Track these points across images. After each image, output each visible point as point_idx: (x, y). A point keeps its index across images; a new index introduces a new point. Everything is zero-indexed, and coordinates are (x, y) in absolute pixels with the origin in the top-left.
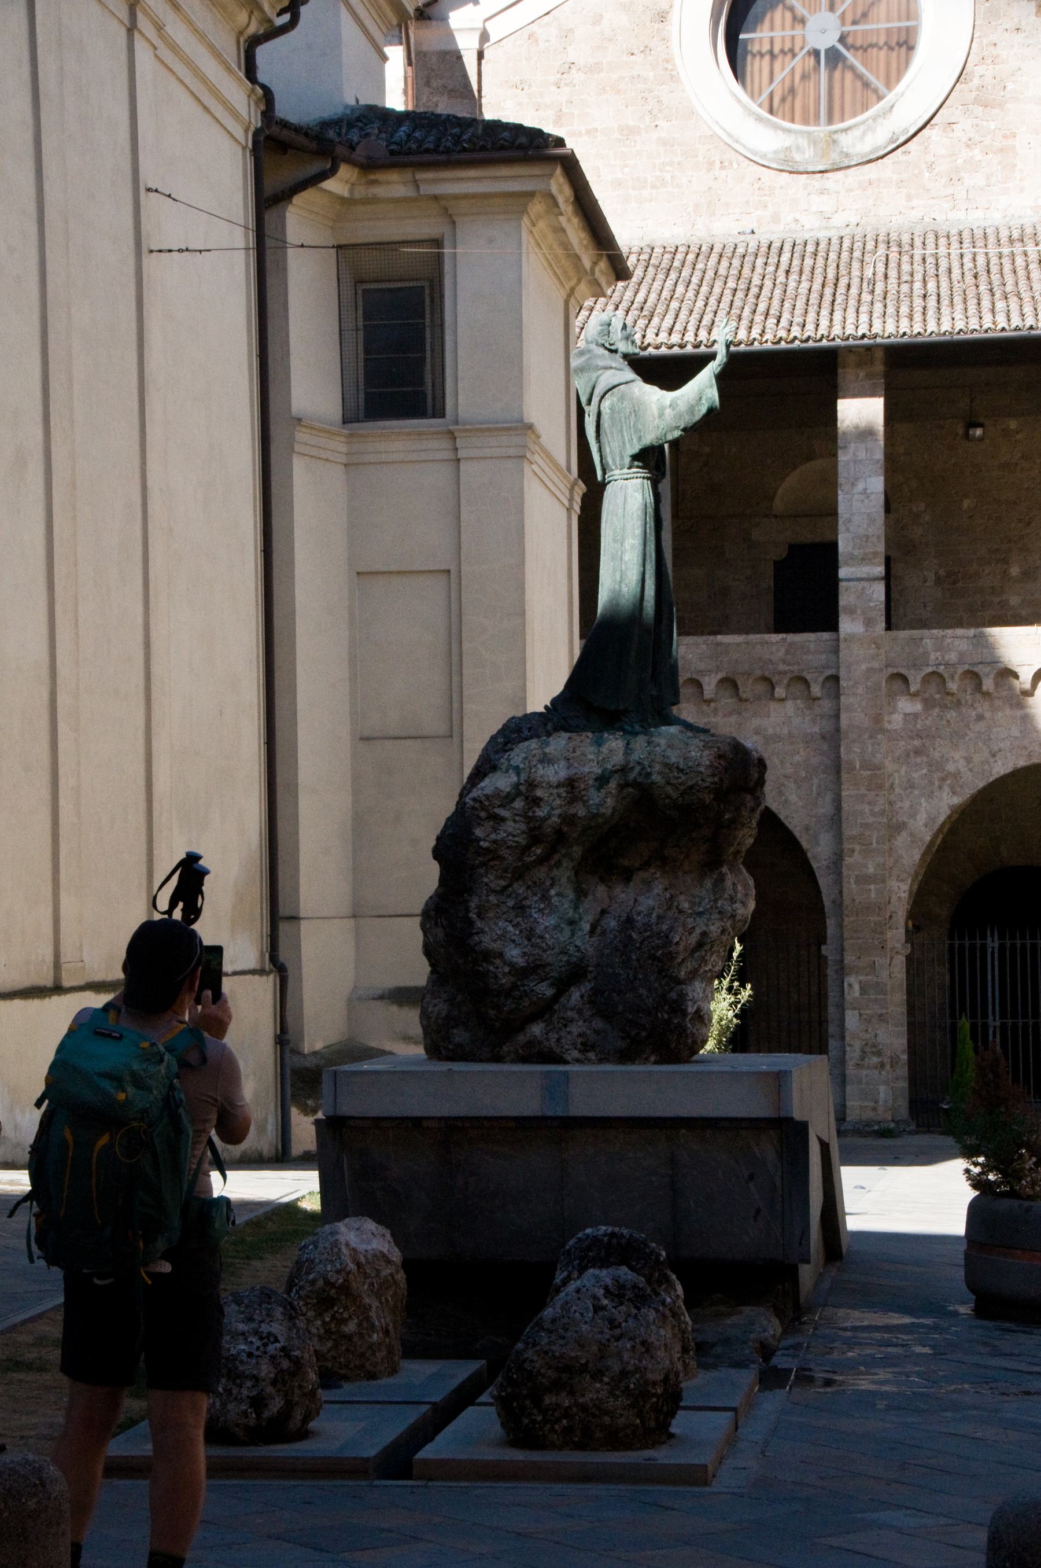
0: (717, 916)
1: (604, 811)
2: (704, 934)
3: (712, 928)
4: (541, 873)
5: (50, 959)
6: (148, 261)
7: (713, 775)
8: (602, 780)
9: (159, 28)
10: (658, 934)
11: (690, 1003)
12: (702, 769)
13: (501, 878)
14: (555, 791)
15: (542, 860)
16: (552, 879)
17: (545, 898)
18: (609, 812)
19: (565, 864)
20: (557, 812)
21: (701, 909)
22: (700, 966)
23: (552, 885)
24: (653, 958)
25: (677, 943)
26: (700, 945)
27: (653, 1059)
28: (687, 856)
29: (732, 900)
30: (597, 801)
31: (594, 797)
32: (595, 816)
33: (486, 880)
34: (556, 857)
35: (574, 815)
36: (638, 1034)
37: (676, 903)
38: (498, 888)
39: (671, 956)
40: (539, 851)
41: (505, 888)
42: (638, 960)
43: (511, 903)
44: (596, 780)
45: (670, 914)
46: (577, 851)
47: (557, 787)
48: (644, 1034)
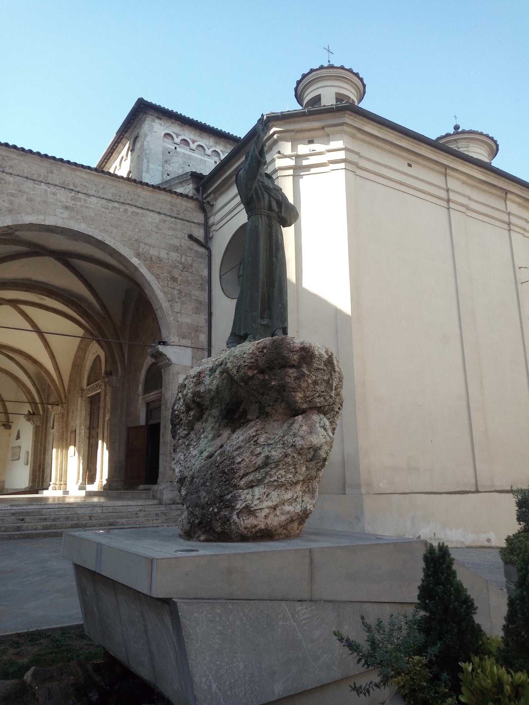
0: (281, 446)
1: (211, 387)
2: (267, 457)
3: (273, 453)
4: (198, 426)
5: (475, 482)
6: (519, 286)
7: (252, 358)
8: (212, 370)
9: (524, 230)
10: (230, 458)
11: (240, 502)
12: (245, 356)
13: (185, 430)
14: (192, 379)
15: (199, 418)
16: (203, 428)
17: (199, 439)
18: (214, 388)
19: (210, 420)
20: (191, 391)
21: (272, 442)
22: (264, 478)
23: (203, 432)
24: (223, 472)
25: (239, 463)
26: (266, 464)
27: (202, 538)
28: (277, 411)
29: (295, 435)
30: (208, 383)
31: (207, 380)
32: (210, 391)
33: (179, 431)
34: (205, 416)
35: (199, 392)
36: (193, 521)
37: (255, 439)
38: (183, 436)
39: (233, 471)
40: (192, 414)
41: (187, 435)
42: (211, 474)
43: (186, 444)
44: (210, 371)
45: (247, 445)
46: (215, 412)
47: (194, 378)
48: (197, 521)
